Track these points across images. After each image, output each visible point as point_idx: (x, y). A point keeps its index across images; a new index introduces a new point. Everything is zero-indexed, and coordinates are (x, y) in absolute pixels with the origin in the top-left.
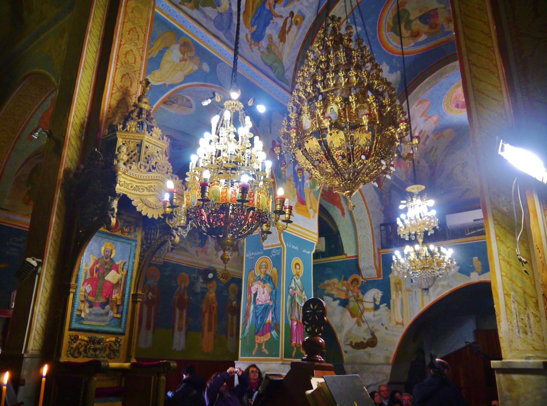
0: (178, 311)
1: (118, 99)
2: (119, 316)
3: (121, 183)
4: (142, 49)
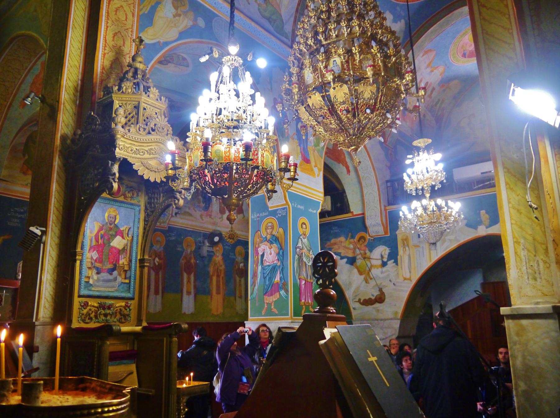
0: (185, 275)
1: (111, 59)
2: (127, 281)
3: (120, 147)
4: (132, 5)
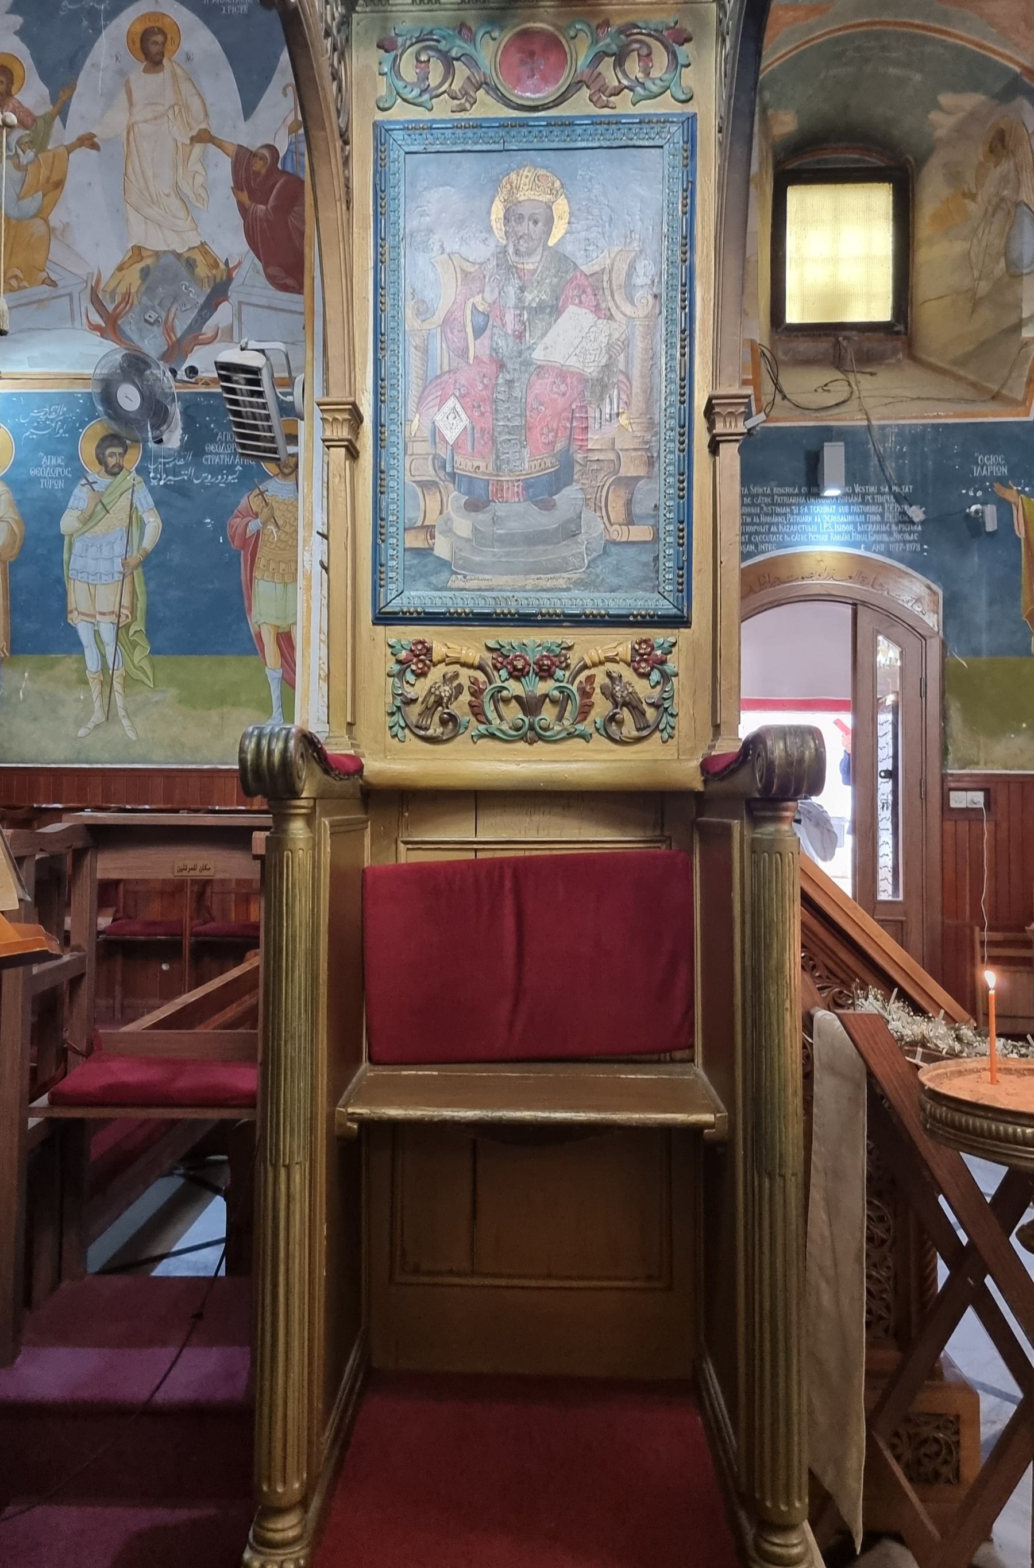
2: (641, 533)
